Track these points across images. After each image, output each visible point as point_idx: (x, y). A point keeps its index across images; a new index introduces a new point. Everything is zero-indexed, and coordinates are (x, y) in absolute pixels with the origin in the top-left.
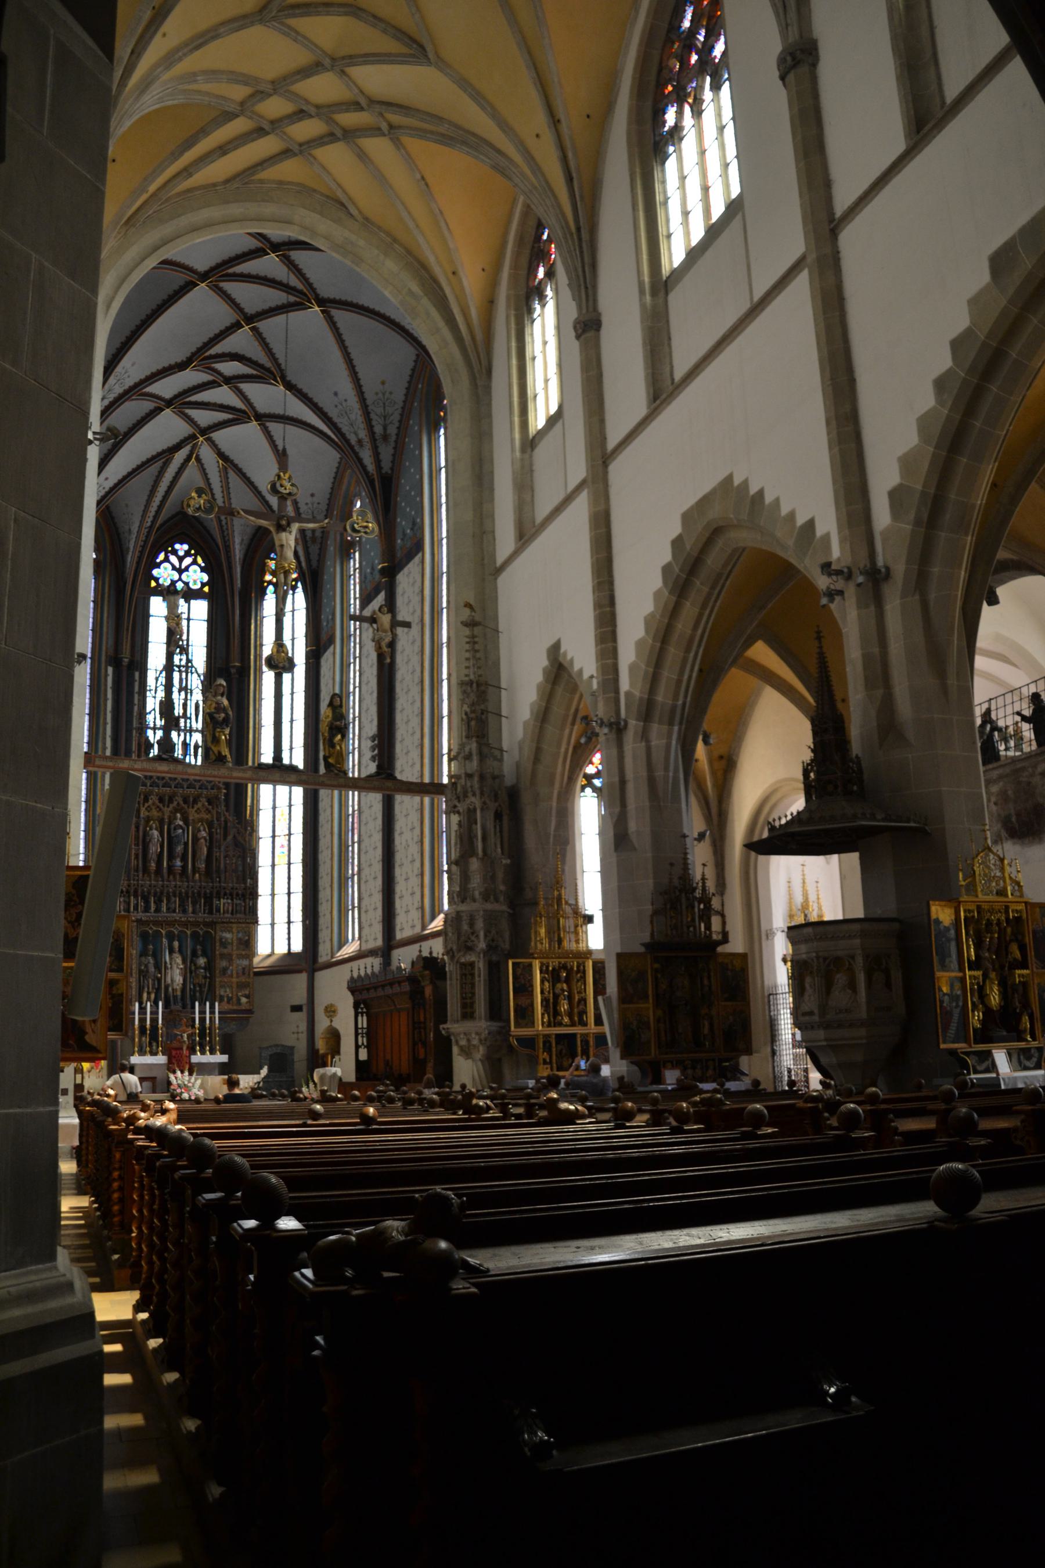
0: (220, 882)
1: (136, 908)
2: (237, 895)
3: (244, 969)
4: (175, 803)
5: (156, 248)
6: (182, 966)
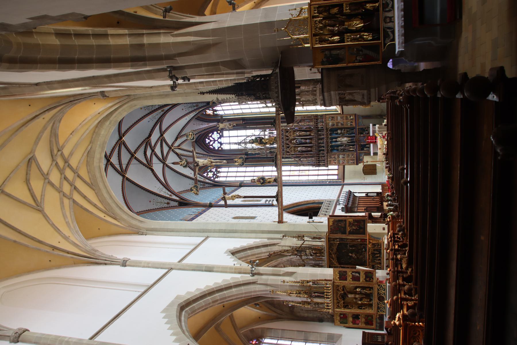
1: (323, 154)
2: (317, 121)
3: (341, 118)
4: (289, 143)
5: (120, 208)
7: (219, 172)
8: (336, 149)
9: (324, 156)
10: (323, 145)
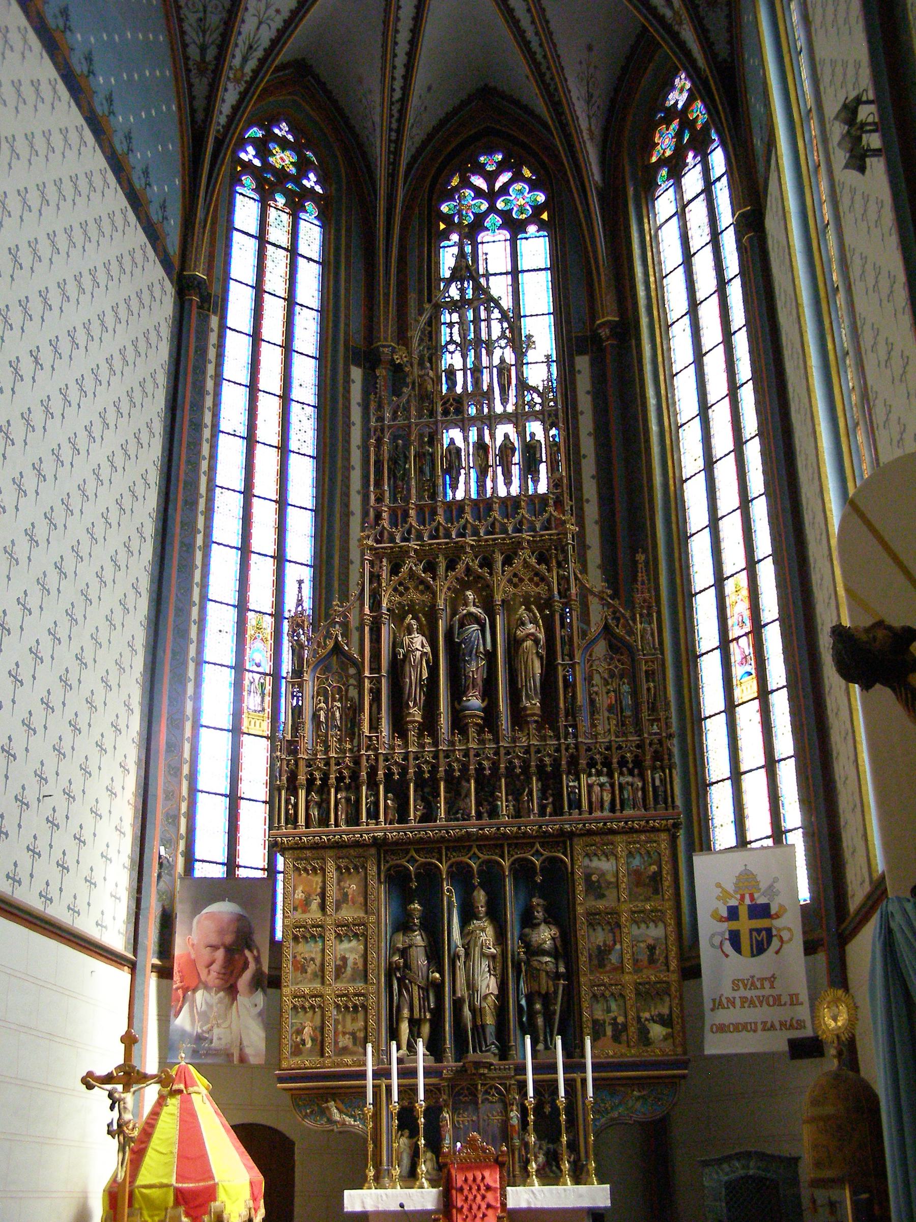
0: (575, 736)
1: (373, 814)
3: (652, 948)
4: (461, 567)
6: (493, 950)
7: (295, 209)
8: (408, 915)
9: (353, 820)
10: (442, 813)
